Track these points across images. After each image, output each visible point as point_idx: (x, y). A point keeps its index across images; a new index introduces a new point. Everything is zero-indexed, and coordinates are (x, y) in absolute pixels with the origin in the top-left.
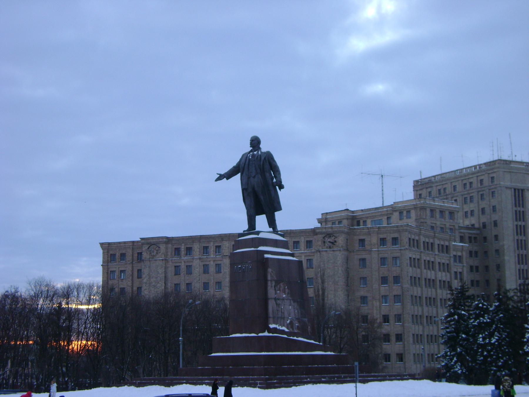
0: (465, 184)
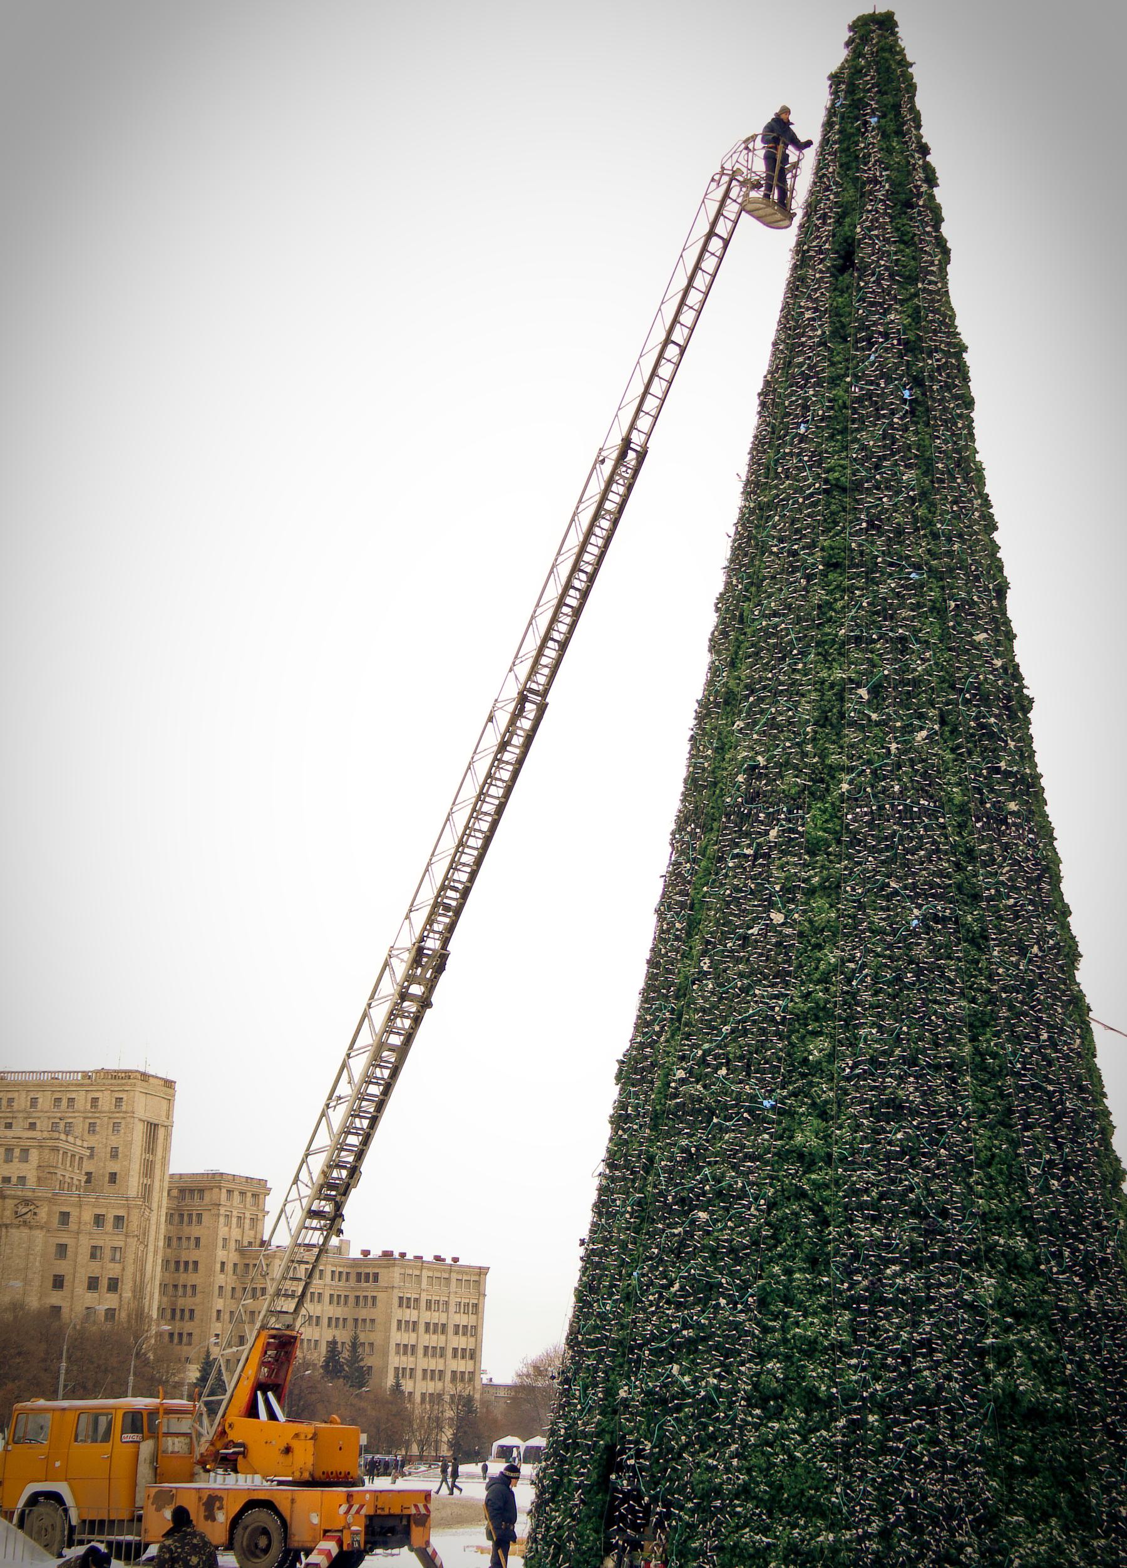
0: (58, 1100)
